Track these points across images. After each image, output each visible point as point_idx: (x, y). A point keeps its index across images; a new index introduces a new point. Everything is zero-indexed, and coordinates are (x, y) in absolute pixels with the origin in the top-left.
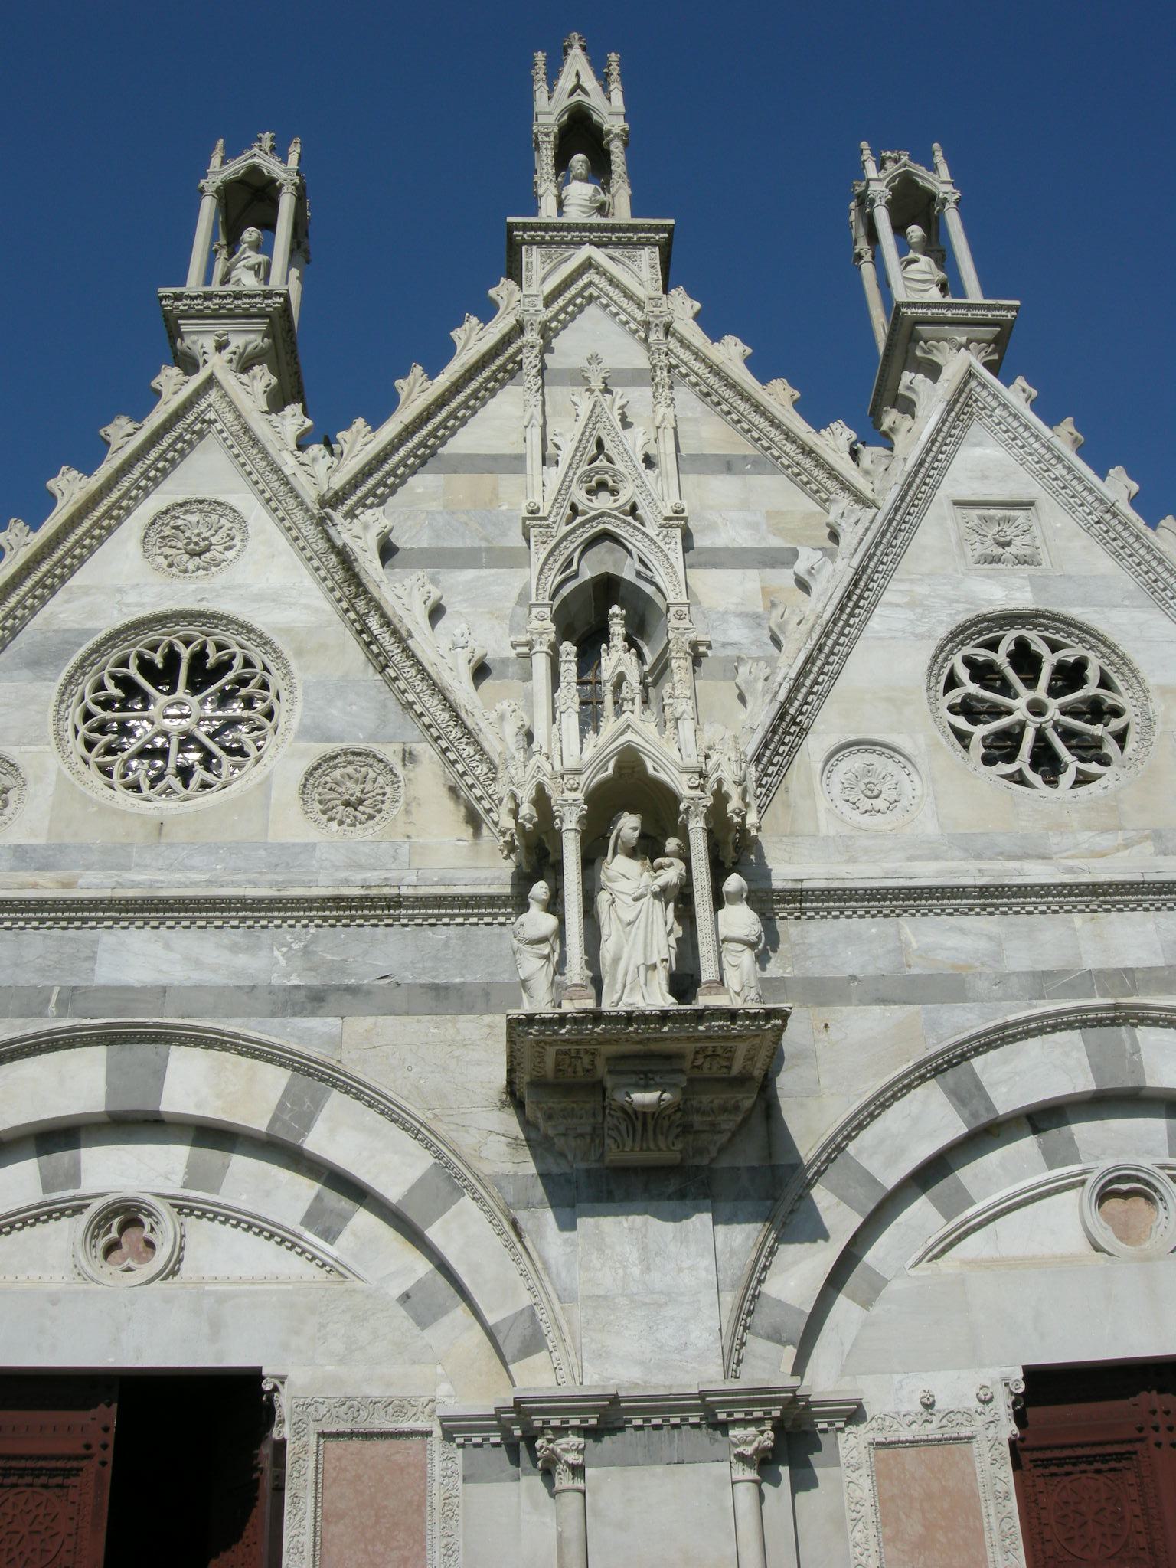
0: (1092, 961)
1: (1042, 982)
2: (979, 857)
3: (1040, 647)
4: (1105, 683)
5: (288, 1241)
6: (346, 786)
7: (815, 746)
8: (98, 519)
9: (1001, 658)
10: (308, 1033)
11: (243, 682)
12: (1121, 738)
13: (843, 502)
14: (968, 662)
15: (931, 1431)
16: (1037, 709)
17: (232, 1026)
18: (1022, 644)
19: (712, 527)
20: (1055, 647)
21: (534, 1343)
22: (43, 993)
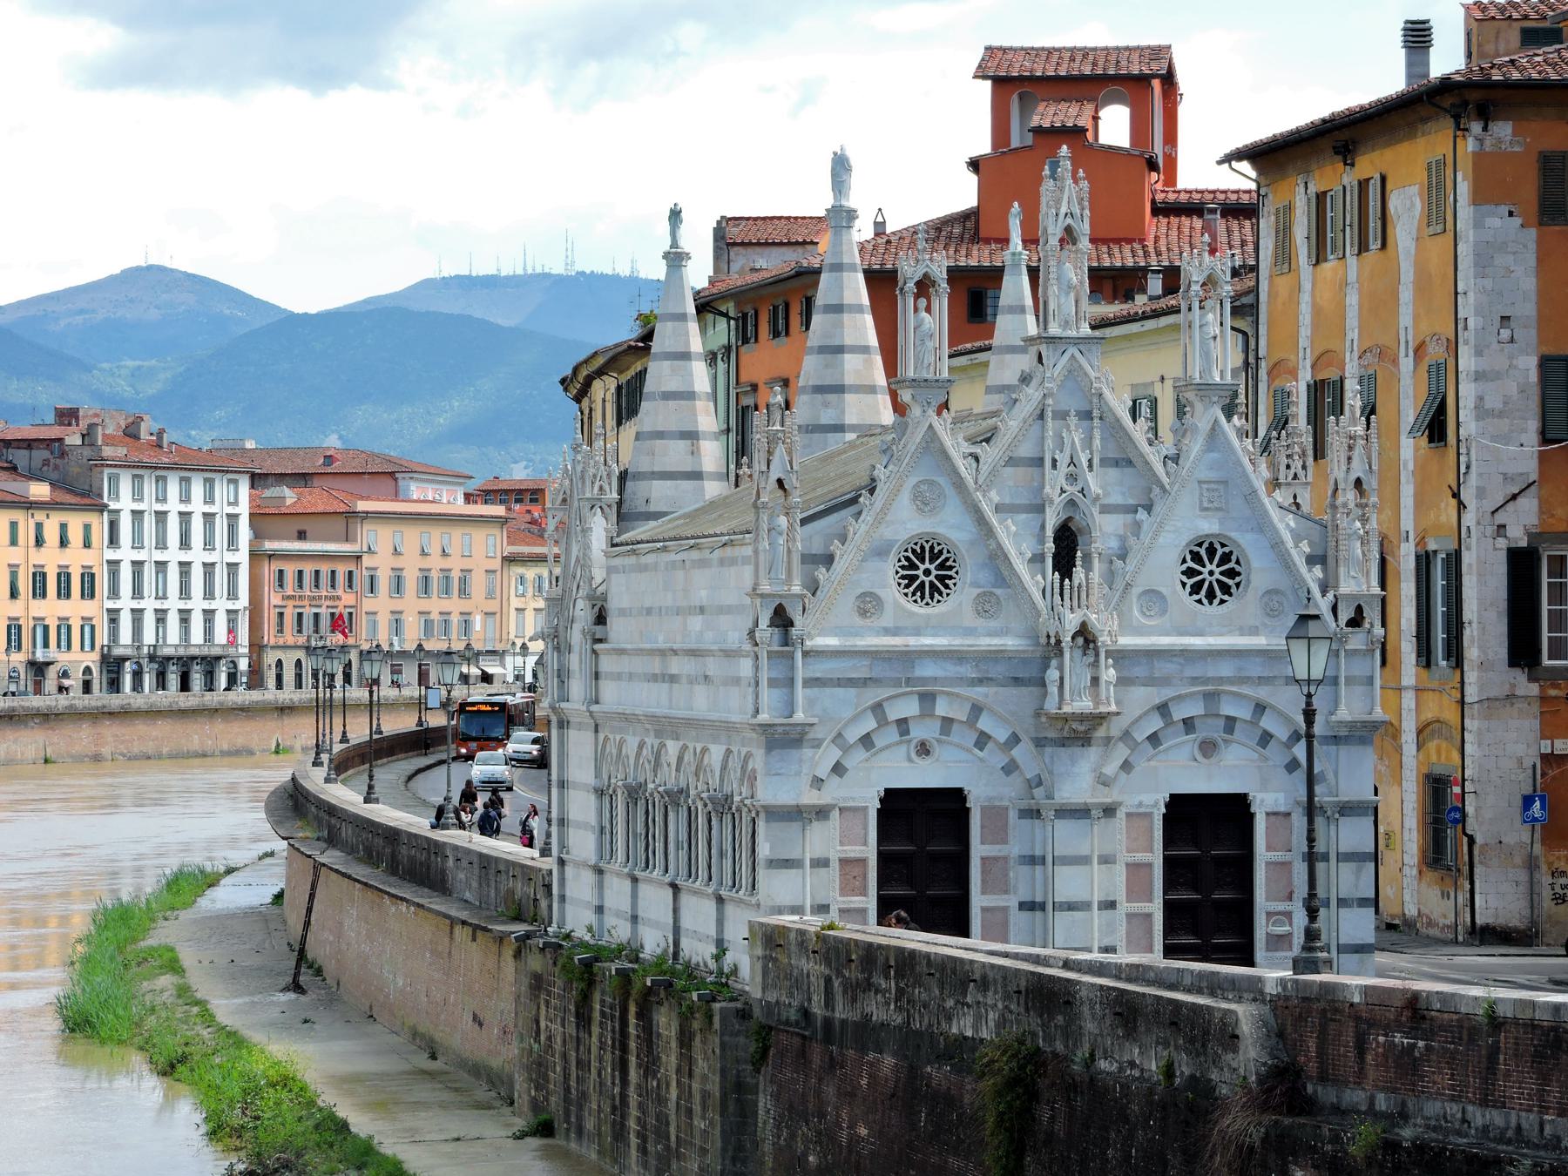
0: (1210, 674)
1: (1194, 680)
2: (1181, 634)
3: (1217, 546)
4: (1238, 562)
5: (969, 751)
6: (985, 605)
7: (1136, 591)
8: (896, 492)
9: (1203, 552)
10: (978, 693)
11: (947, 559)
12: (1238, 585)
13: (1157, 490)
14: (1191, 552)
15: (1142, 810)
16: (1211, 573)
17: (956, 690)
18: (1211, 544)
19: (1106, 494)
20: (1223, 545)
21: (1040, 784)
22: (899, 679)
